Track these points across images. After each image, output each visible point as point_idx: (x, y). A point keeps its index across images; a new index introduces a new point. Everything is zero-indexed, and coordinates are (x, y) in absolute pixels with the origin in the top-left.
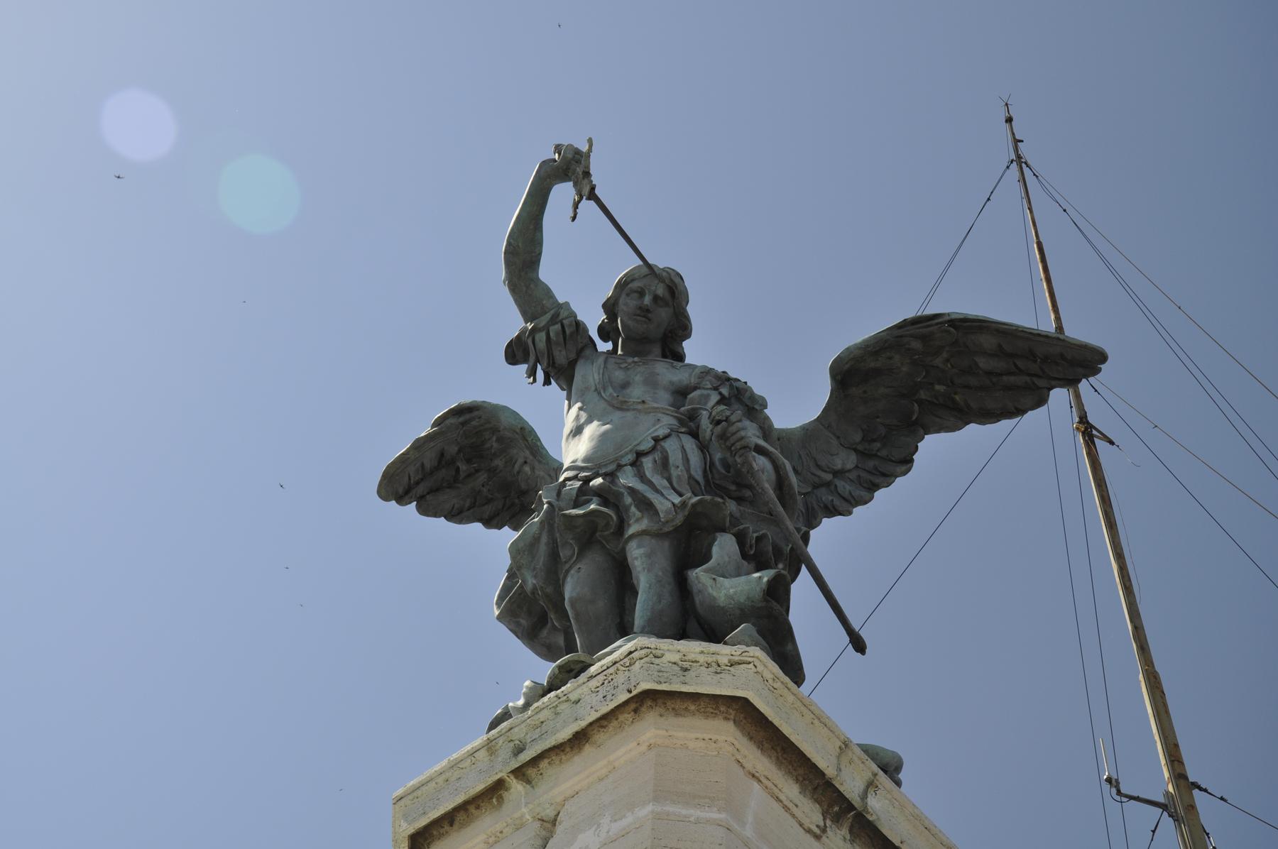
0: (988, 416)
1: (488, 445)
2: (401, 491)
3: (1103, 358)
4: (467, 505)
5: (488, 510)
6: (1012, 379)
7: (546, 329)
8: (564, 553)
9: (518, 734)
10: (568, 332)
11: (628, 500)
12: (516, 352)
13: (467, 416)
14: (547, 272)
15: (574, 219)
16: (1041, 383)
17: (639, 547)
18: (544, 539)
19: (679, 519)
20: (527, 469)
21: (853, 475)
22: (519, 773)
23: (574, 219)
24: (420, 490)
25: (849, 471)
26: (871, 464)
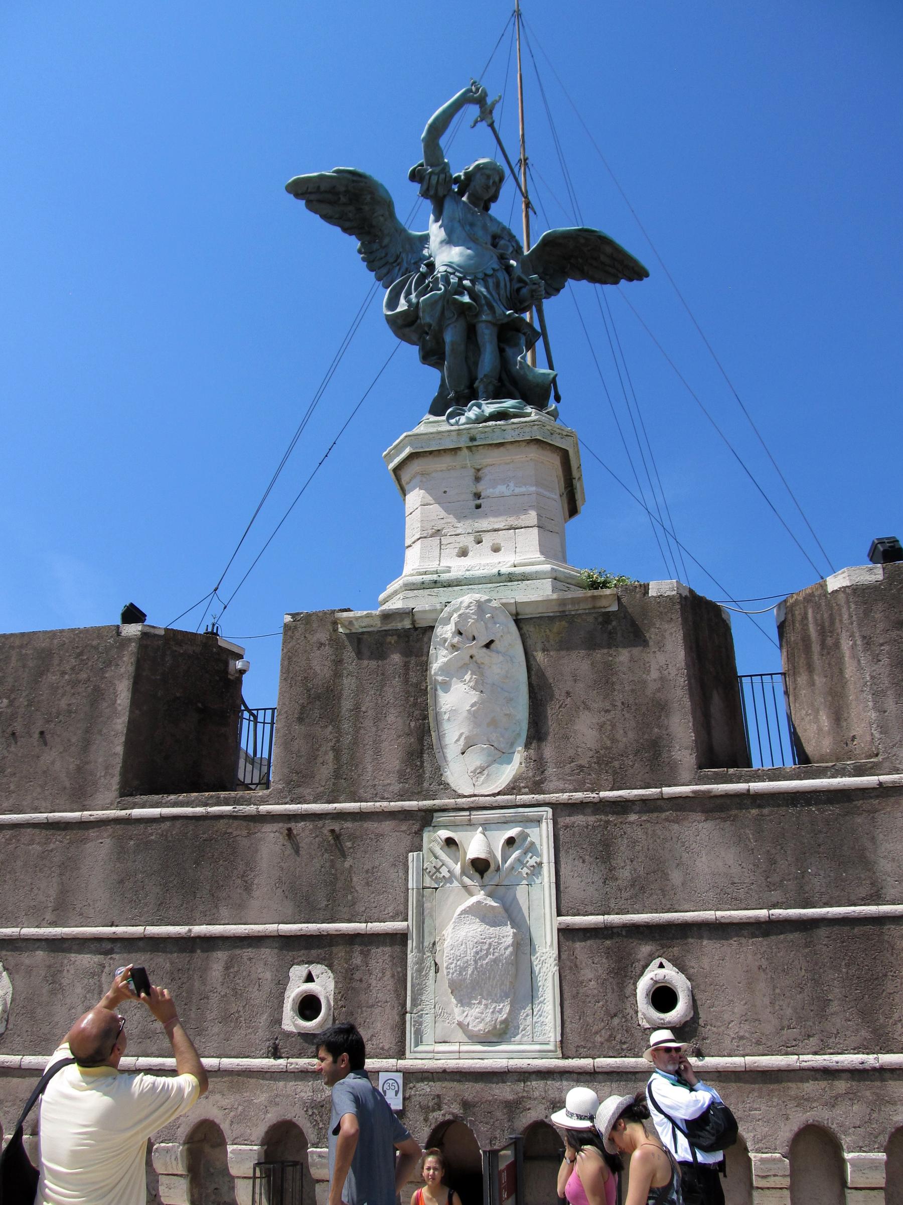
0: (593, 279)
2: (300, 192)
3: (647, 275)
4: (337, 216)
7: (438, 174)
8: (448, 314)
9: (473, 432)
11: (483, 302)
12: (415, 176)
13: (359, 179)
14: (443, 142)
16: (620, 275)
19: (505, 320)
20: (382, 219)
22: (469, 448)
24: (312, 197)
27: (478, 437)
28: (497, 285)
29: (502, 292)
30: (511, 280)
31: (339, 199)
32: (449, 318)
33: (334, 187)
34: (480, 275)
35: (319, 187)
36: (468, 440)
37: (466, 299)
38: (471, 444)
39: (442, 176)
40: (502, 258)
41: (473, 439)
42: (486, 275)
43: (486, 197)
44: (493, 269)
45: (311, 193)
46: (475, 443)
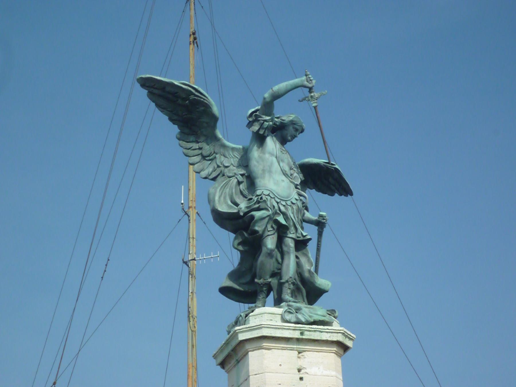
1: (197, 107)
2: (147, 85)
3: (352, 194)
4: (168, 109)
6: (332, 186)
11: (292, 224)
15: (299, 101)
16: (336, 191)
19: (302, 238)
20: (205, 125)
23: (299, 101)
27: (306, 333)
34: (289, 203)
35: (164, 88)
36: (299, 334)
37: (283, 222)
38: (301, 337)
41: (302, 334)
46: (304, 337)
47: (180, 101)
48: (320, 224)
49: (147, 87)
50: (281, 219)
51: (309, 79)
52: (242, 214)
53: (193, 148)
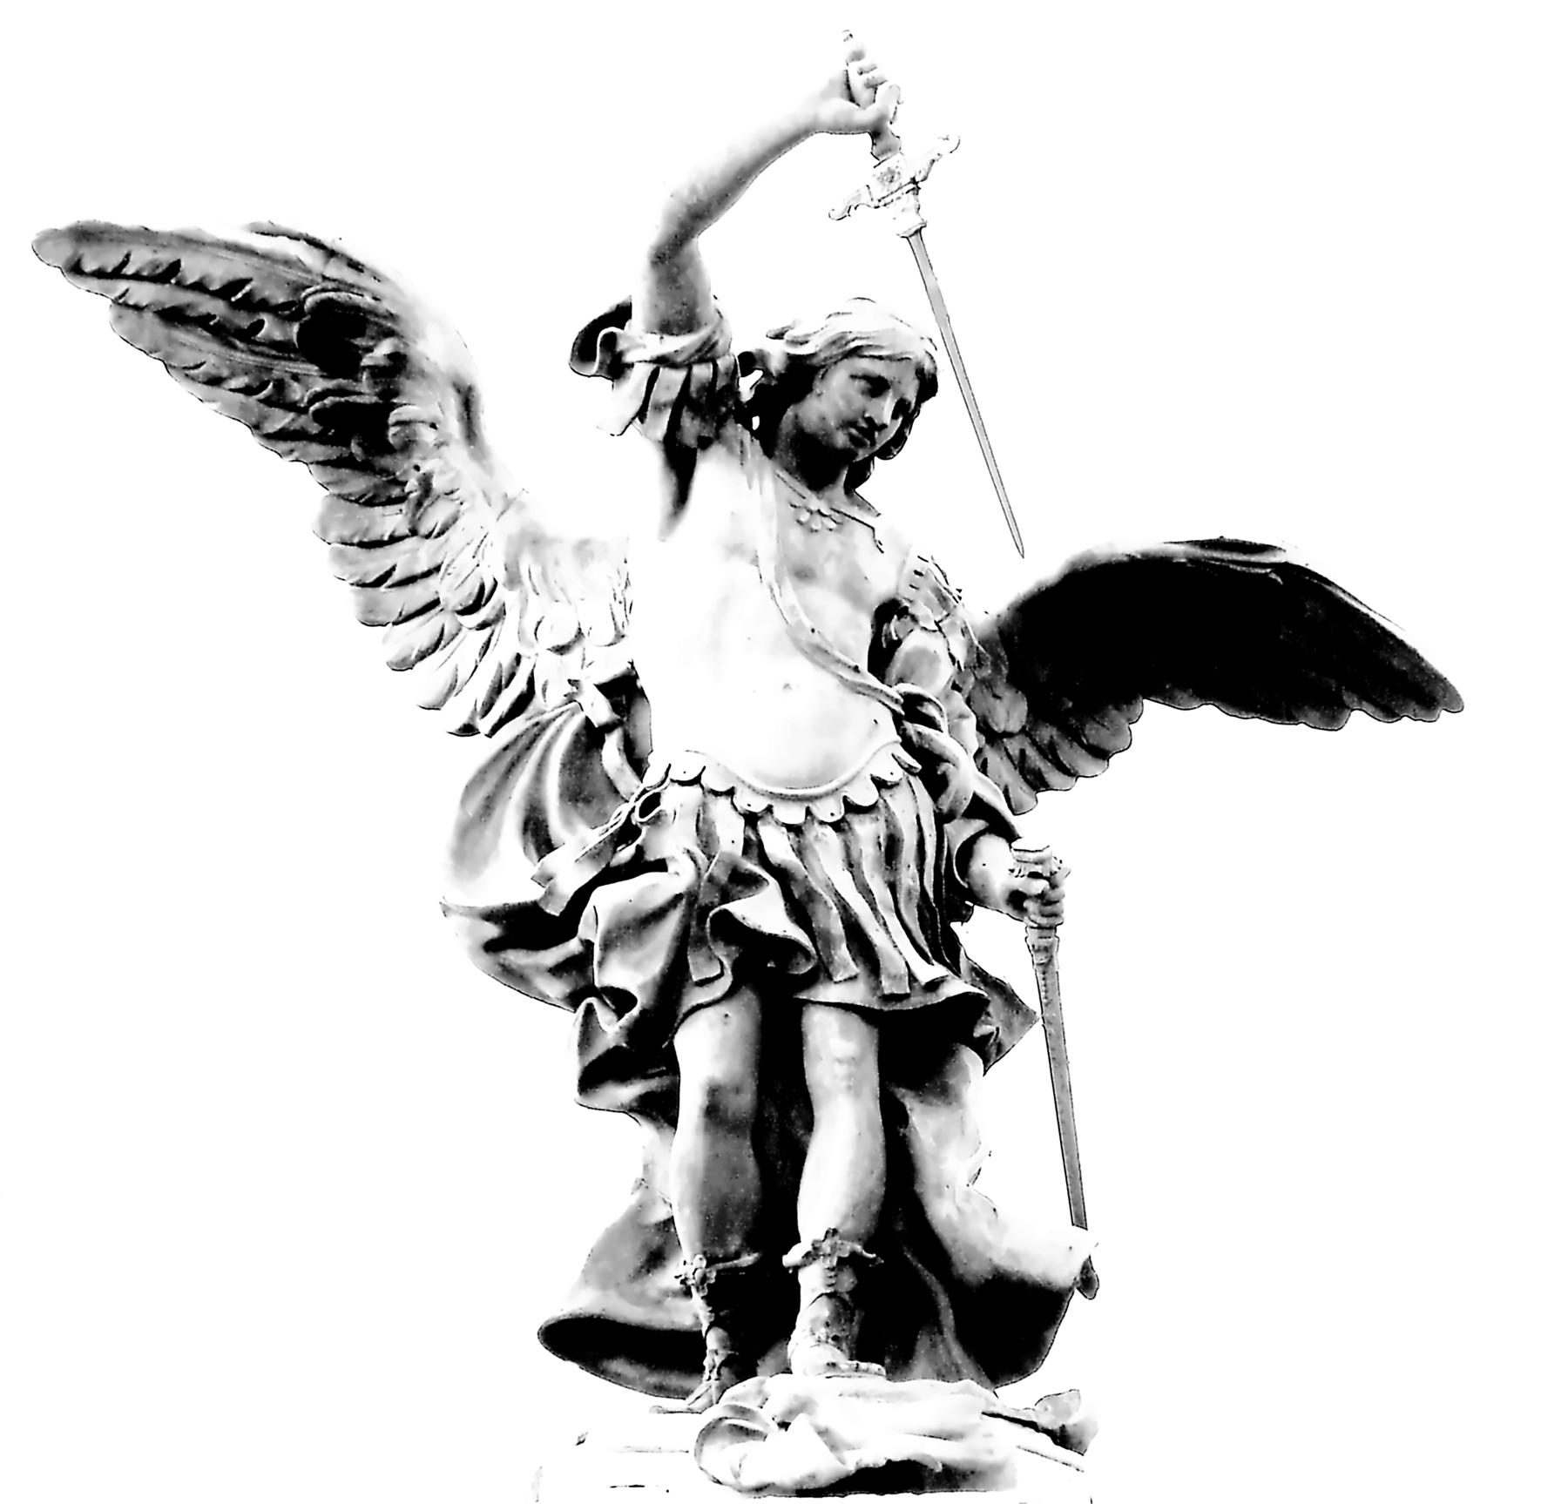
2: (89, 266)
4: (234, 383)
5: (281, 420)
10: (721, 383)
11: (837, 928)
13: (350, 276)
17: (844, 1033)
18: (670, 926)
21: (1014, 747)
24: (143, 293)
25: (1010, 735)
26: (1047, 733)
28: (891, 849)
29: (908, 877)
30: (942, 819)
31: (261, 323)
32: (703, 983)
33: (240, 283)
34: (830, 810)
35: (175, 267)
39: (702, 372)
40: (912, 709)
42: (851, 808)
43: (862, 454)
44: (880, 784)
45: (137, 277)
47: (270, 328)
48: (1037, 904)
49: (100, 274)
50: (763, 911)
51: (857, 83)
52: (554, 910)
53: (396, 576)
